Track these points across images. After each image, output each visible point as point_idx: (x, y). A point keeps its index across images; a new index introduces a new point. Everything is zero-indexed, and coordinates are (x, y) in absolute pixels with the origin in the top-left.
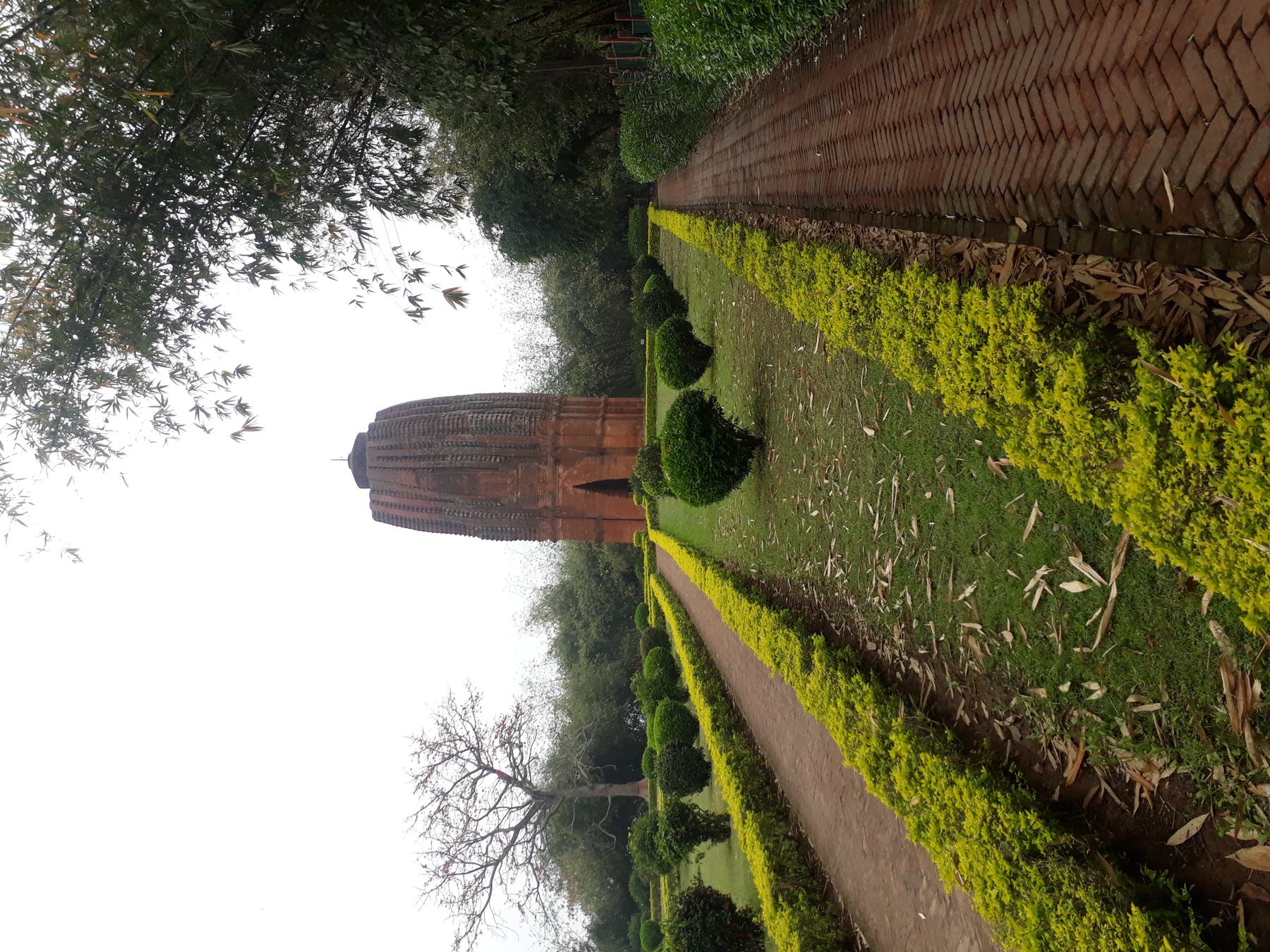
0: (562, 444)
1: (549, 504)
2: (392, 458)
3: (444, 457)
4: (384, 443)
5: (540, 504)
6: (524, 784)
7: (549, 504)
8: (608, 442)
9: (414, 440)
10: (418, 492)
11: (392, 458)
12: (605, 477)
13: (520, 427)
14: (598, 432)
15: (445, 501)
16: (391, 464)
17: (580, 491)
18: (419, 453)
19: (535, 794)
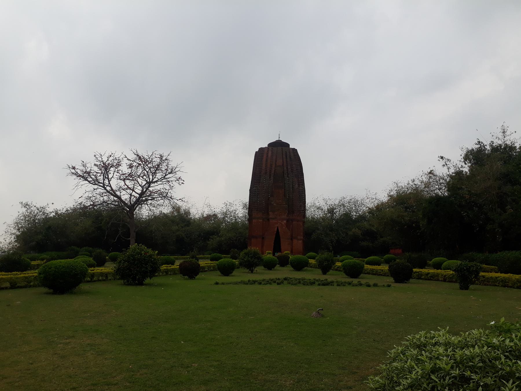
0: (294, 223)
1: (270, 217)
2: (286, 157)
3: (288, 176)
4: (292, 155)
5: (270, 213)
6: (139, 201)
7: (270, 217)
8: (295, 241)
9: (294, 166)
10: (274, 166)
11: (286, 157)
12: (282, 240)
13: (301, 206)
14: (299, 237)
15: (270, 175)
16: (284, 156)
17: (276, 229)
18: (289, 167)
19: (132, 207)
